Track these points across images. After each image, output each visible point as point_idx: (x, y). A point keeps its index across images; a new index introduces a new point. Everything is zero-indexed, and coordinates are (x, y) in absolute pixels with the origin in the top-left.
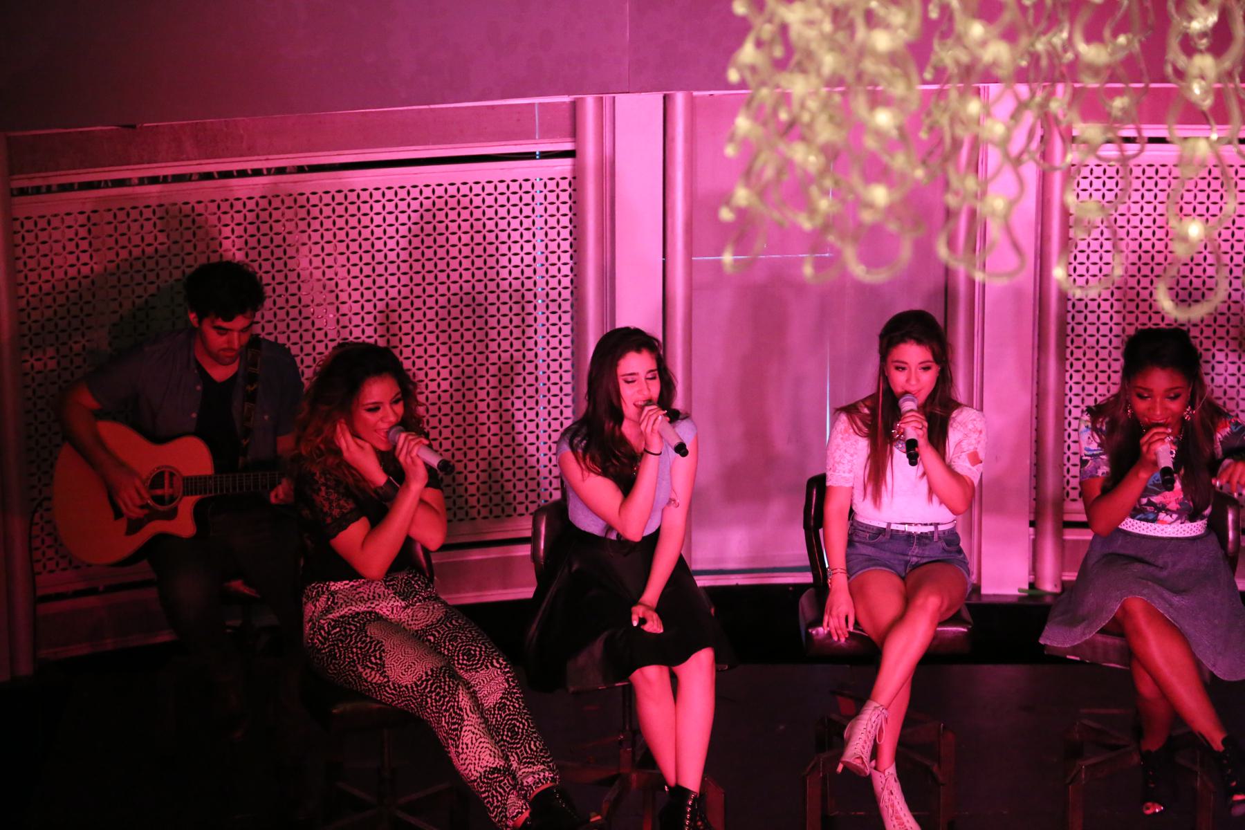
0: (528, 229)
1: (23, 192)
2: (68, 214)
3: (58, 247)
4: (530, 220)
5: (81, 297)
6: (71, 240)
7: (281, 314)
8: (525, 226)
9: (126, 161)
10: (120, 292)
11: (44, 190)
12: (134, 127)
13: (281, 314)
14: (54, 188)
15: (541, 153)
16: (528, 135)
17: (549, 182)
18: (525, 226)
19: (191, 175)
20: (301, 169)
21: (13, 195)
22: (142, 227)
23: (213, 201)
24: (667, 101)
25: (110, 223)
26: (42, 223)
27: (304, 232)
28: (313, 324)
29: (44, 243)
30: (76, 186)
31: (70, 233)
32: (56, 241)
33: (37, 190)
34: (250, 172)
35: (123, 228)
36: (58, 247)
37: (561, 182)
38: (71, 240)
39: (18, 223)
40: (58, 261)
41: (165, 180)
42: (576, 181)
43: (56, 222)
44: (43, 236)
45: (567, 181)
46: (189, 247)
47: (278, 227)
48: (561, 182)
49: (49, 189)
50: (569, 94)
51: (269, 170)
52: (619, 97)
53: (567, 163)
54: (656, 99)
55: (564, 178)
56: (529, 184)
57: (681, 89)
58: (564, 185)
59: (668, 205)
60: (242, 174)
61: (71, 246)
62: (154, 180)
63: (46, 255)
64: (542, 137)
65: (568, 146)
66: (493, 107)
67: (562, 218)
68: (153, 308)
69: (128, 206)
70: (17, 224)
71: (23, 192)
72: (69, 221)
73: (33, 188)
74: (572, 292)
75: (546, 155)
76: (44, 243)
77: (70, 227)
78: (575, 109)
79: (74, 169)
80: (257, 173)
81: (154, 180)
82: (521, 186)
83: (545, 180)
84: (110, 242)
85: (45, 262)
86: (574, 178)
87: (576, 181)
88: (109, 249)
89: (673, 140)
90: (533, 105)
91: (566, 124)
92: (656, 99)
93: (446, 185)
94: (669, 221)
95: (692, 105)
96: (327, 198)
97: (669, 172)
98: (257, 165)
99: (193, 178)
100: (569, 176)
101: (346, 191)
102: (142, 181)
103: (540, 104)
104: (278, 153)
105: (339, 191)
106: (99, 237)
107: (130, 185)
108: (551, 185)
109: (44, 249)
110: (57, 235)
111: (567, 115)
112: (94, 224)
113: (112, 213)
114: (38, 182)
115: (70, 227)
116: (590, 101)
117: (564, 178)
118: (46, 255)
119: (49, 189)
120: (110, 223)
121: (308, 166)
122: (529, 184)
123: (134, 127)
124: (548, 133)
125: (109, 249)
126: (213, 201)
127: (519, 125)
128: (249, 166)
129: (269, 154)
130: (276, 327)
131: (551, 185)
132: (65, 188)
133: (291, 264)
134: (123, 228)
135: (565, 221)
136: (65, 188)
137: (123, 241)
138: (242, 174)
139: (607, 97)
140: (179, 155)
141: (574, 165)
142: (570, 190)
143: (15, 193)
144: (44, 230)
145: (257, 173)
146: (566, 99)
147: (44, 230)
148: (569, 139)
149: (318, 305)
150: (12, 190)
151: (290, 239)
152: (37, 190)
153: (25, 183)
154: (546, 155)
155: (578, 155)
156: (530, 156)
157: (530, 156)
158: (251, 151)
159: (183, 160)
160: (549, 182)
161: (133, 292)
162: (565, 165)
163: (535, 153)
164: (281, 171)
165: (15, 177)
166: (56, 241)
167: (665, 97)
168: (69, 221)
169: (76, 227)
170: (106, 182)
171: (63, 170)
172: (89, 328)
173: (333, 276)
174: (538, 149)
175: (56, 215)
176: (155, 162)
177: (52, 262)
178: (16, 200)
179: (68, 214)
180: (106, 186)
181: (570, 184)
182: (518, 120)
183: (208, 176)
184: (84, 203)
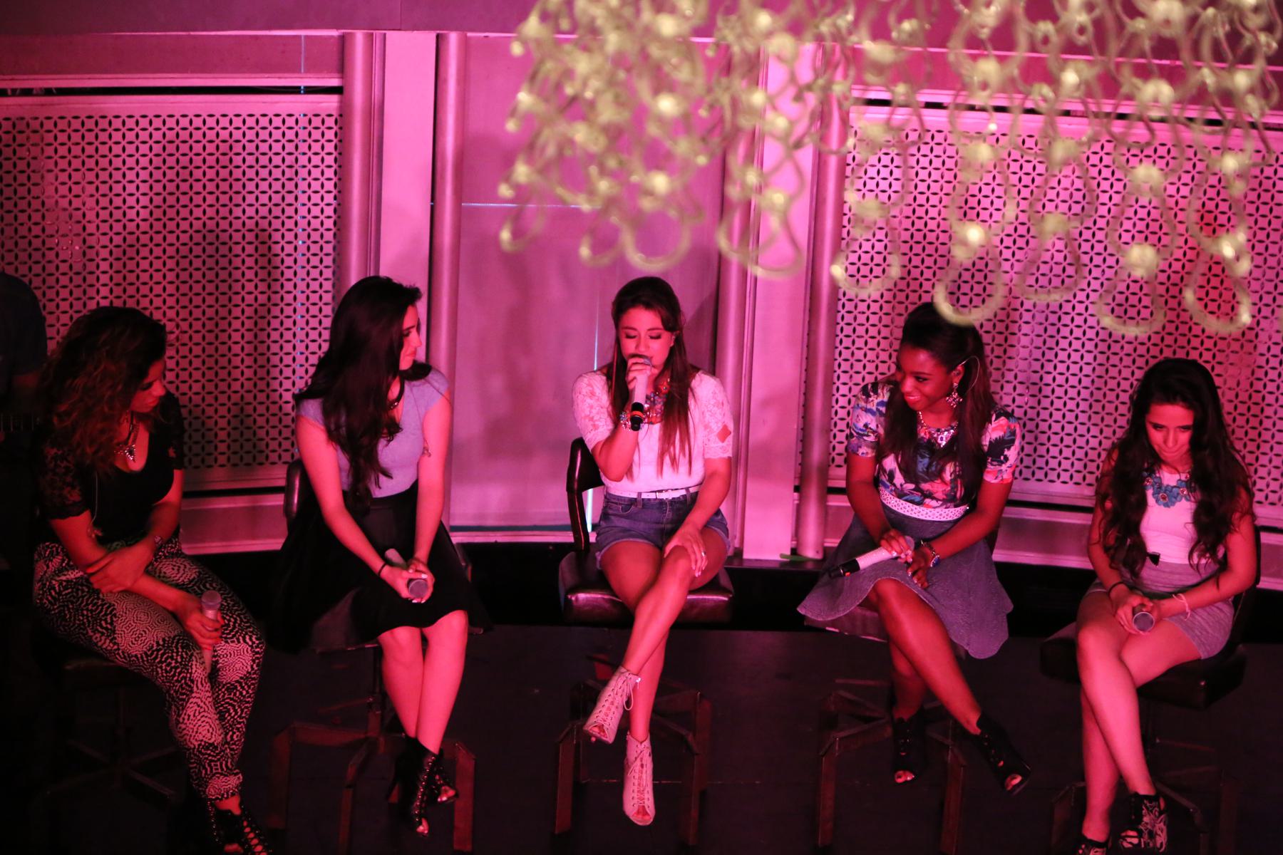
0: (290, 167)
4: (293, 158)
8: (287, 163)
15: (306, 87)
16: (294, 69)
18: (287, 163)
24: (440, 41)
27: (50, 158)
28: (57, 255)
37: (327, 119)
42: (343, 118)
45: (332, 119)
47: (22, 152)
48: (327, 119)
50: (338, 28)
52: (391, 35)
54: (429, 38)
55: (330, 115)
56: (293, 119)
57: (456, 29)
58: (330, 122)
59: (439, 149)
64: (307, 71)
65: (334, 82)
66: (256, 37)
67: (326, 157)
74: (335, 234)
78: (343, 44)
82: (284, 122)
83: (310, 115)
86: (341, 115)
87: (343, 118)
89: (446, 81)
90: (299, 37)
92: (429, 38)
93: (204, 116)
94: (439, 165)
95: (465, 45)
97: (440, 115)
100: (335, 113)
103: (307, 37)
104: (25, 74)
105: (90, 117)
108: (317, 122)
116: (359, 36)
117: (330, 115)
121: (56, 89)
122: (293, 119)
124: (313, 68)
127: (284, 57)
129: (16, 74)
131: (317, 122)
133: (36, 191)
135: (330, 160)
139: (377, 33)
141: (341, 102)
142: (335, 128)
146: (334, 33)
148: (337, 75)
149: (63, 236)
156: (294, 90)
157: (294, 90)
162: (331, 102)
163: (299, 87)
164: (27, 92)
167: (438, 36)
173: (81, 206)
174: (303, 83)
181: (336, 122)
182: (283, 52)
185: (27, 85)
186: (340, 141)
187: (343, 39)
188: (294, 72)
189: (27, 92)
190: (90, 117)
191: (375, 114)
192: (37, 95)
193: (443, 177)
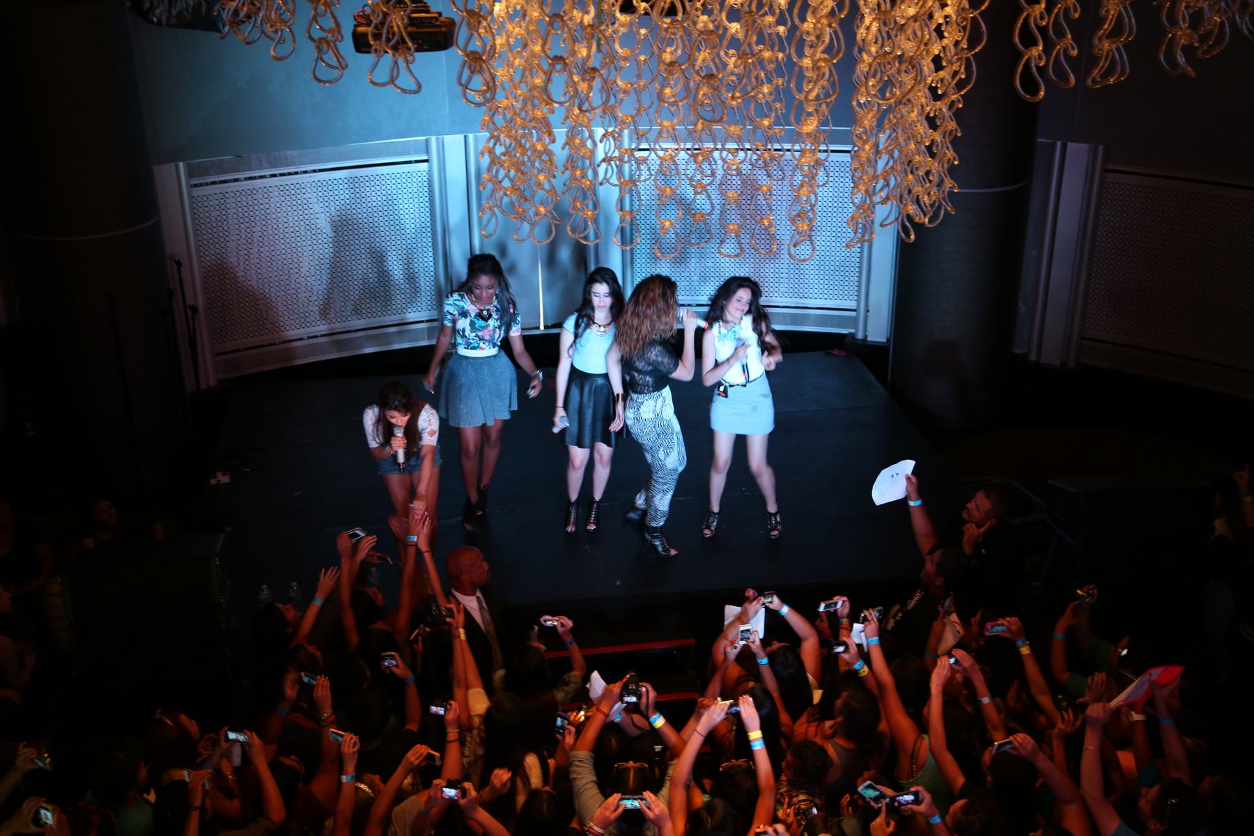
1: (196, 186)
3: (212, 209)
9: (237, 171)
16: (409, 154)
20: (315, 171)
33: (201, 185)
35: (239, 199)
40: (213, 214)
41: (255, 178)
42: (430, 171)
46: (267, 206)
49: (207, 184)
50: (424, 136)
53: (426, 164)
58: (425, 174)
60: (290, 174)
62: (251, 178)
69: (240, 189)
71: (196, 186)
72: (216, 197)
78: (427, 142)
80: (296, 173)
81: (251, 178)
87: (430, 171)
91: (424, 148)
98: (295, 170)
102: (246, 179)
109: (206, 209)
110: (211, 203)
111: (424, 144)
114: (202, 181)
116: (433, 139)
119: (207, 184)
124: (417, 152)
127: (405, 150)
128: (292, 170)
132: (214, 183)
136: (214, 183)
138: (290, 174)
139: (440, 137)
140: (261, 168)
145: (296, 173)
152: (201, 185)
153: (197, 182)
156: (410, 162)
157: (410, 162)
158: (293, 164)
162: (424, 166)
164: (305, 172)
167: (465, 136)
168: (216, 197)
178: (194, 189)
183: (275, 176)
185: (305, 169)
187: (427, 140)
189: (305, 172)
191: (442, 169)
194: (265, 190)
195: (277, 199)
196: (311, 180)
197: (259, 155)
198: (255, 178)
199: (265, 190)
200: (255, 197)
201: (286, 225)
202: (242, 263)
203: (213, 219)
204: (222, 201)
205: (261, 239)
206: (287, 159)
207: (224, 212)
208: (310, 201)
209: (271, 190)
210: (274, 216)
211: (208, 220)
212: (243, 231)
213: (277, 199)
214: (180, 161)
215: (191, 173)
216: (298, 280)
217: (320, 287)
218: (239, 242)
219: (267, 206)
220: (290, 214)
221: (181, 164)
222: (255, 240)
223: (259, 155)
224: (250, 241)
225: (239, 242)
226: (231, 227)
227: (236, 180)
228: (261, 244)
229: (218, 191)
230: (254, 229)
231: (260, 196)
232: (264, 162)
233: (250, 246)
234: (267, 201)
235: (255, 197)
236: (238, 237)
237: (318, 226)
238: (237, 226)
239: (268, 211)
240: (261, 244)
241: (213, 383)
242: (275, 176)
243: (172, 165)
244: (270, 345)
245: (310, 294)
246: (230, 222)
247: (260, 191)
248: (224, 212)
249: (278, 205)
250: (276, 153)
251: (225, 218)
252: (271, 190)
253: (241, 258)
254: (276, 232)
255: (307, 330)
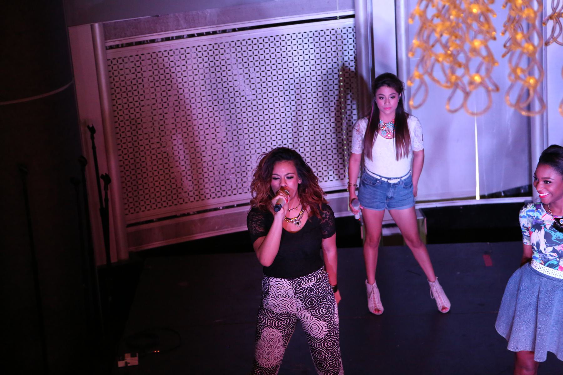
2: (131, 56)
3: (127, 71)
5: (138, 92)
6: (133, 67)
7: (226, 96)
10: (155, 90)
11: (120, 46)
12: (158, 16)
13: (226, 96)
14: (124, 45)
15: (340, 16)
16: (334, 9)
17: (343, 30)
19: (183, 36)
20: (234, 30)
21: (107, 49)
22: (163, 60)
23: (194, 47)
25: (149, 59)
26: (120, 61)
29: (121, 69)
30: (134, 44)
31: (133, 65)
32: (127, 69)
34: (211, 32)
36: (127, 71)
38: (133, 67)
39: (110, 61)
40: (128, 77)
41: (172, 39)
43: (126, 60)
44: (121, 67)
46: (184, 68)
49: (122, 46)
51: (219, 31)
55: (350, 27)
61: (133, 70)
62: (168, 39)
63: (122, 75)
64: (340, 9)
65: (351, 13)
68: (170, 96)
70: (110, 62)
71: (111, 47)
72: (132, 59)
73: (115, 45)
75: (342, 17)
76: (121, 69)
77: (132, 62)
79: (133, 36)
81: (168, 39)
84: (150, 68)
85: (122, 78)
86: (355, 27)
88: (150, 71)
89: (399, 7)
96: (244, 43)
97: (398, 22)
99: (185, 37)
101: (252, 39)
102: (163, 40)
105: (249, 39)
106: (145, 66)
107: (158, 42)
110: (126, 66)
112: (143, 60)
113: (150, 55)
114: (117, 43)
115: (132, 62)
117: (350, 27)
118: (122, 75)
120: (149, 59)
123: (158, 16)
124: (342, 8)
125: (150, 71)
126: (194, 47)
130: (224, 102)
134: (155, 61)
137: (155, 67)
143: (108, 48)
144: (121, 64)
147: (121, 64)
148: (352, 9)
150: (106, 47)
151: (228, 62)
154: (342, 17)
155: (356, 16)
156: (335, 18)
157: (335, 18)
159: (180, 29)
160: (343, 30)
161: (161, 89)
162: (350, 21)
163: (337, 17)
164: (224, 31)
165: (108, 41)
166: (127, 69)
168: (132, 59)
169: (135, 62)
170: (147, 41)
171: (128, 36)
172: (143, 106)
174: (338, 14)
175: (126, 57)
176: (168, 31)
177: (125, 78)
179: (131, 56)
180: (148, 43)
183: (192, 36)
184: (138, 51)
186: (355, 38)
188: (333, 10)
189: (224, 31)
190: (249, 39)
192: (219, 33)
193: (401, 50)
194: (182, 51)
195: (195, 61)
196: (230, 40)
197: (177, 14)
198: (172, 39)
199: (182, 51)
200: (171, 58)
201: (203, 88)
202: (157, 129)
203: (129, 83)
204: (138, 64)
205: (176, 103)
206: (205, 18)
207: (139, 75)
208: (228, 62)
209: (188, 51)
210: (191, 78)
211: (123, 84)
212: (158, 95)
213: (195, 61)
214: (96, 22)
215: (106, 36)
216: (214, 147)
217: (237, 154)
218: (154, 107)
219: (184, 68)
220: (207, 76)
221: (97, 25)
222: (171, 104)
223: (177, 14)
224: (165, 105)
225: (154, 107)
226: (147, 91)
227: (153, 41)
228: (177, 109)
229: (134, 54)
230: (169, 93)
231: (178, 58)
232: (182, 22)
233: (166, 111)
234: (184, 62)
235: (171, 58)
236: (154, 101)
237: (236, 89)
238: (153, 90)
239: (185, 74)
240: (177, 109)
241: (124, 255)
242: (192, 36)
243: (88, 26)
244: (184, 215)
245: (227, 161)
246: (146, 86)
247: (177, 52)
248: (139, 75)
249: (195, 67)
250: (194, 12)
251: (140, 81)
252: (188, 51)
253: (156, 123)
254: (192, 95)
255: (222, 200)
